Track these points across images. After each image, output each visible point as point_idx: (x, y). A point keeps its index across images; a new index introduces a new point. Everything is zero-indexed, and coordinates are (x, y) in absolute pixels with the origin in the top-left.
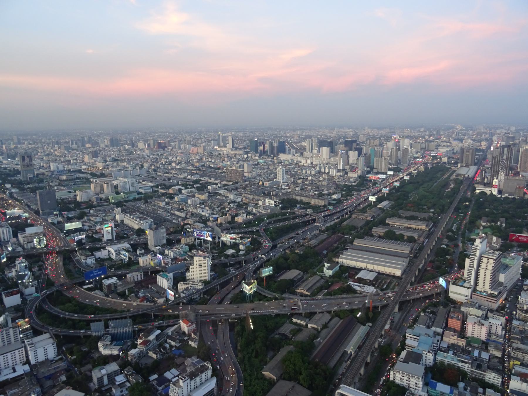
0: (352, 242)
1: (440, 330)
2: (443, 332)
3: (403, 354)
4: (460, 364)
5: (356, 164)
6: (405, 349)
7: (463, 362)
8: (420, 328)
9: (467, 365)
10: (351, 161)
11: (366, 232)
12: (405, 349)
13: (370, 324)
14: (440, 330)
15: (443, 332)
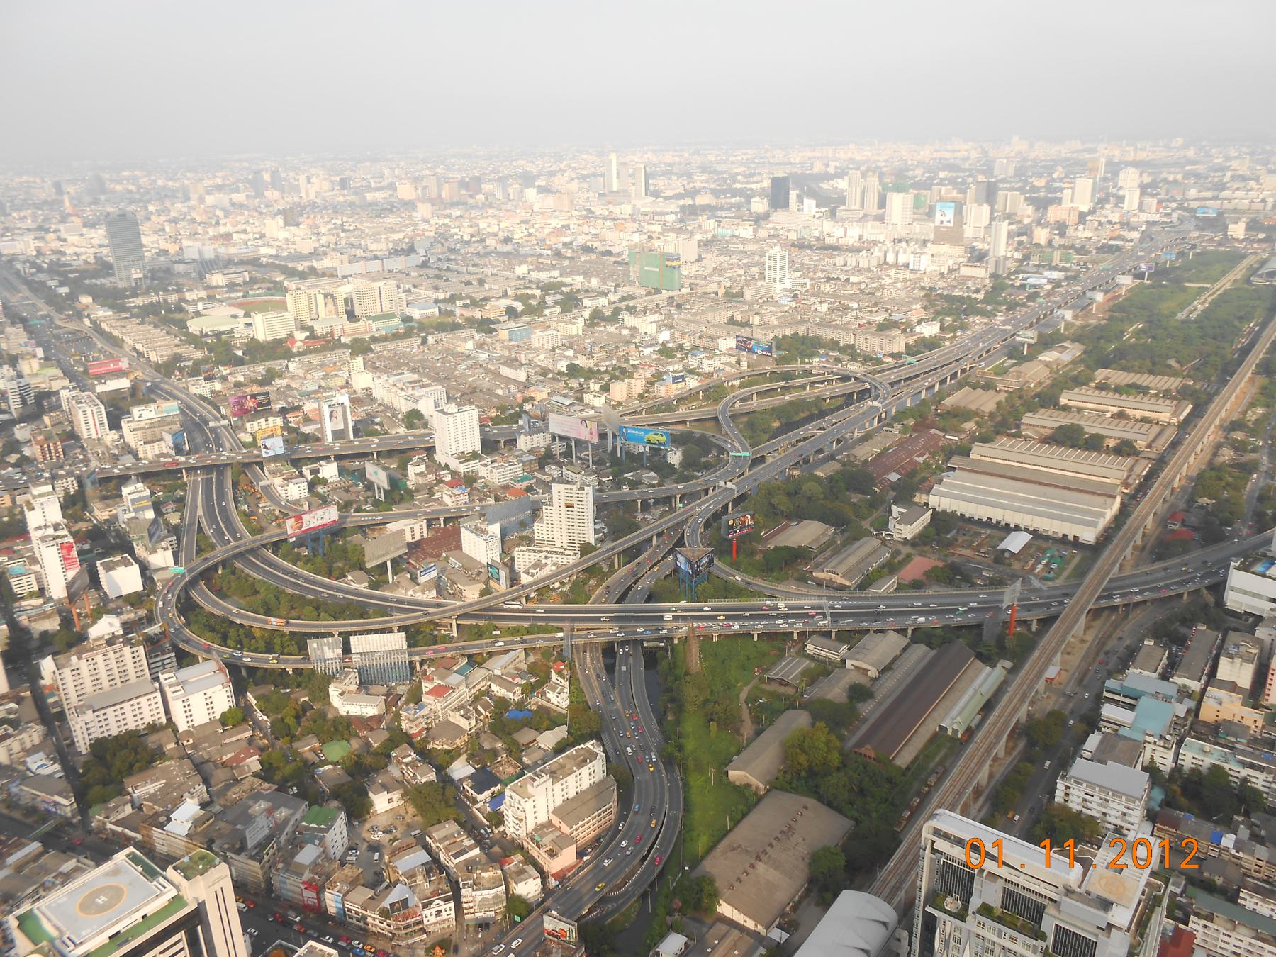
0: (966, 452)
1: (1195, 686)
2: (1203, 691)
3: (1093, 741)
4: (1245, 772)
5: (984, 240)
6: (1099, 729)
7: (1252, 766)
8: (1140, 677)
9: (1262, 776)
10: (969, 232)
11: (1004, 424)
12: (1099, 729)
13: (1008, 664)
14: (1195, 686)
15: (1203, 691)
